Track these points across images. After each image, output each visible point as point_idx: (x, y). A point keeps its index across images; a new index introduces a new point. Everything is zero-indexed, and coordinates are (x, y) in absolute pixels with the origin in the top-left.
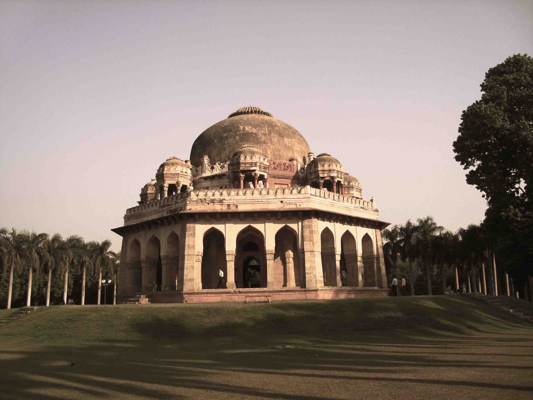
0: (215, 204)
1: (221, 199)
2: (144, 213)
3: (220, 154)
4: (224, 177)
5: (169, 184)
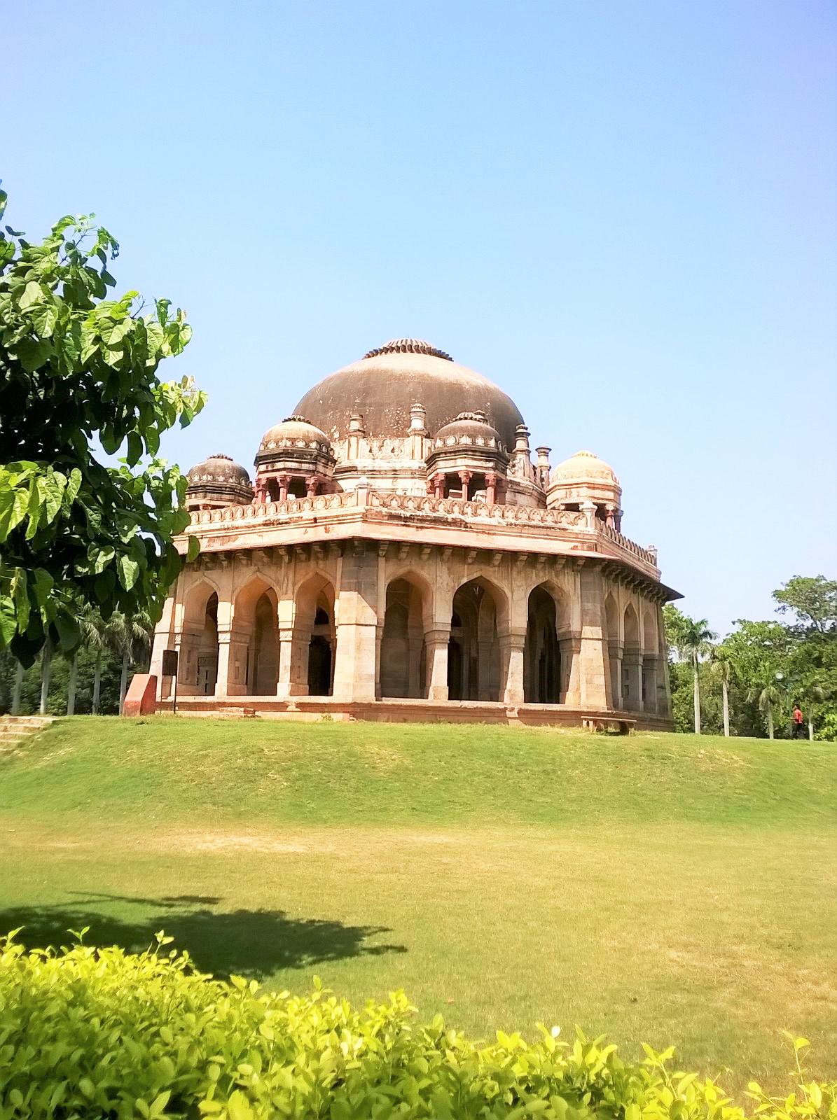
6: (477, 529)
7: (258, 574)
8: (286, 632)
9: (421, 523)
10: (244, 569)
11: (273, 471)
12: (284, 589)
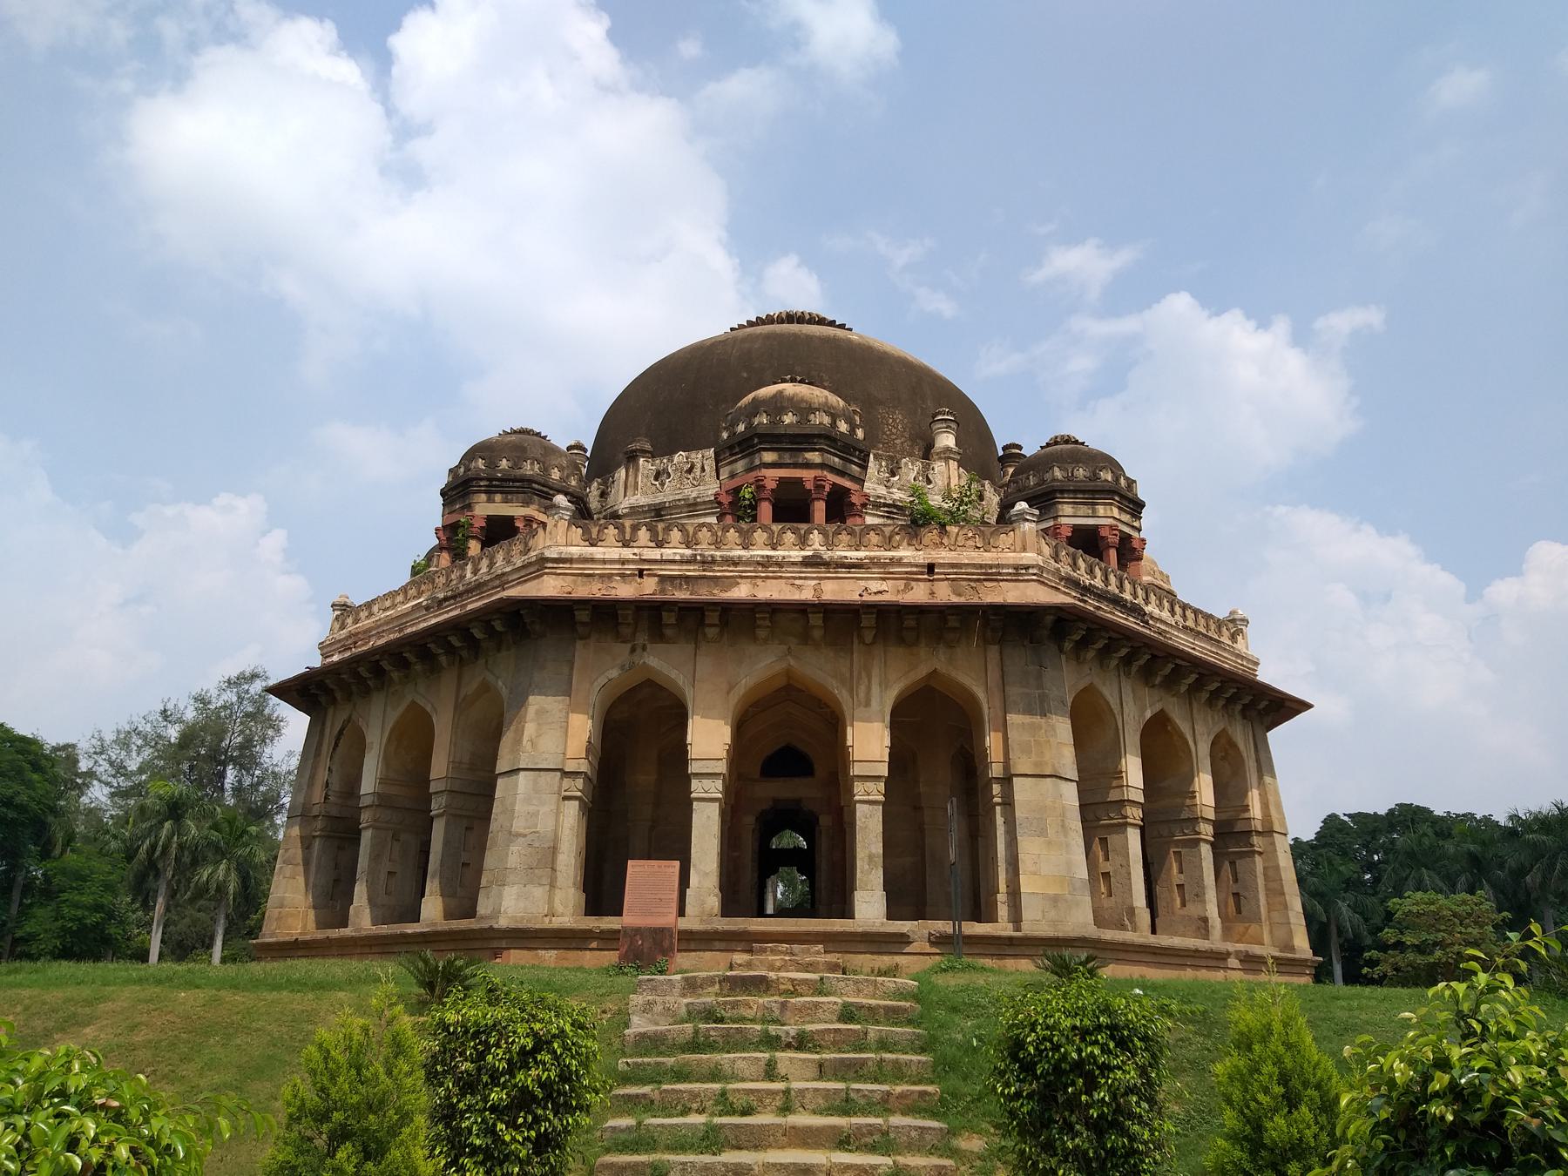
6: (1153, 626)
7: (792, 662)
8: (870, 786)
9: (1098, 602)
11: (796, 466)
12: (862, 695)
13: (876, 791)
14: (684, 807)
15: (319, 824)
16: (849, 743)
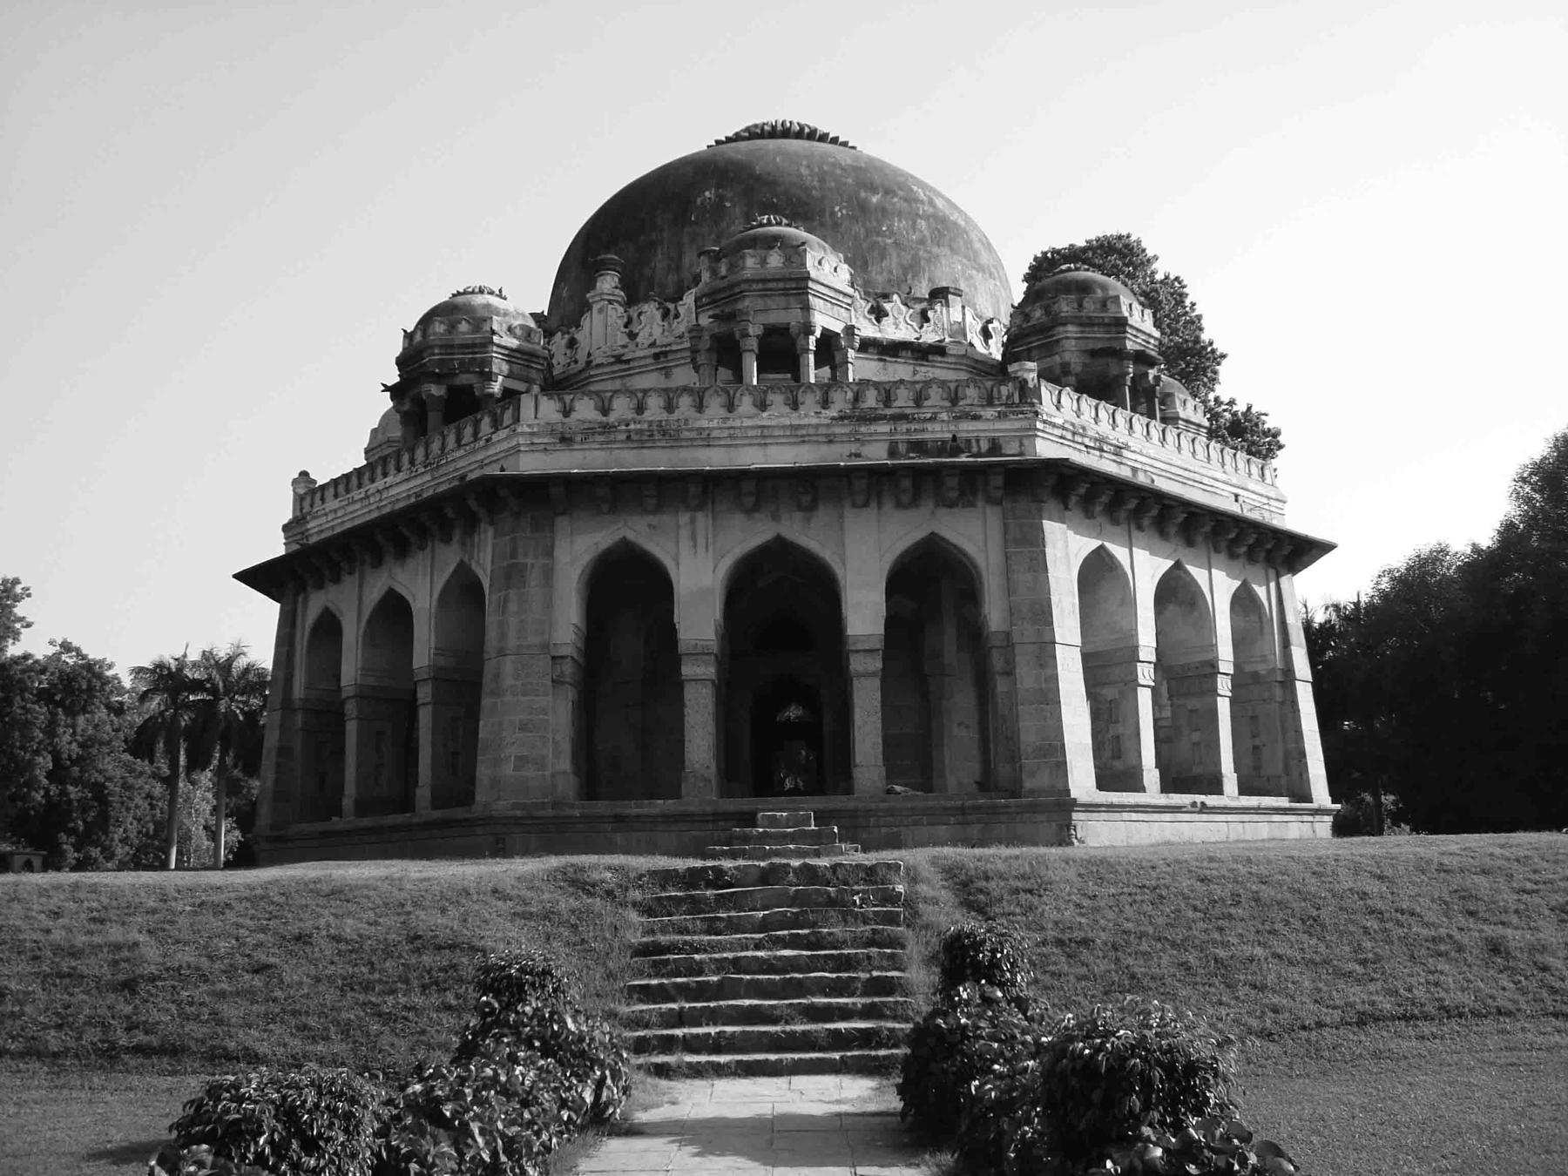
0: (1105, 454)
1: (1121, 440)
2: (700, 430)
3: (866, 263)
4: (940, 359)
5: (824, 328)
10: (738, 519)
13: (876, 664)
14: (679, 685)
15: (299, 719)
16: (844, 615)
